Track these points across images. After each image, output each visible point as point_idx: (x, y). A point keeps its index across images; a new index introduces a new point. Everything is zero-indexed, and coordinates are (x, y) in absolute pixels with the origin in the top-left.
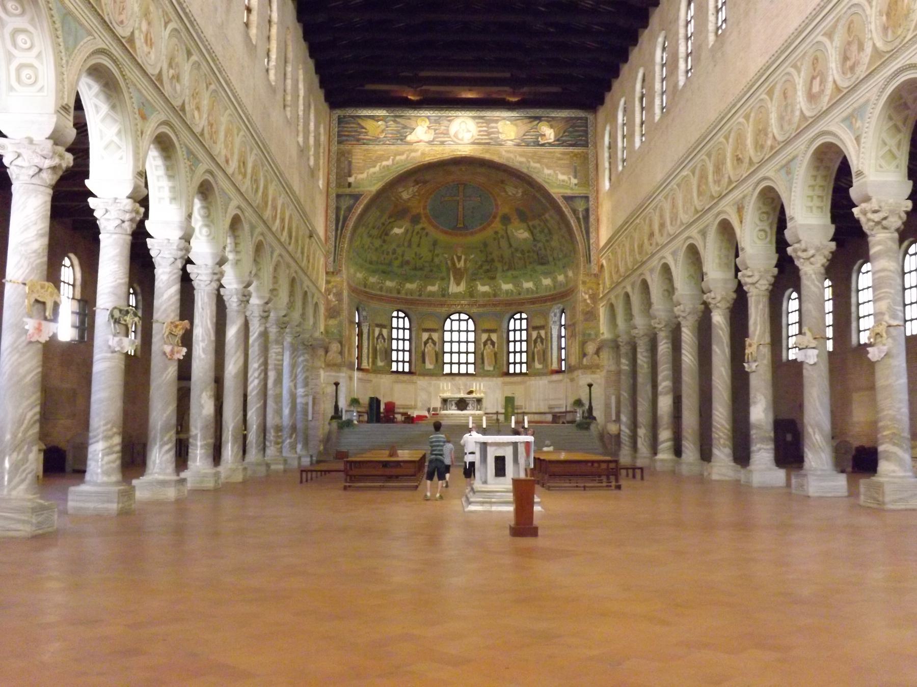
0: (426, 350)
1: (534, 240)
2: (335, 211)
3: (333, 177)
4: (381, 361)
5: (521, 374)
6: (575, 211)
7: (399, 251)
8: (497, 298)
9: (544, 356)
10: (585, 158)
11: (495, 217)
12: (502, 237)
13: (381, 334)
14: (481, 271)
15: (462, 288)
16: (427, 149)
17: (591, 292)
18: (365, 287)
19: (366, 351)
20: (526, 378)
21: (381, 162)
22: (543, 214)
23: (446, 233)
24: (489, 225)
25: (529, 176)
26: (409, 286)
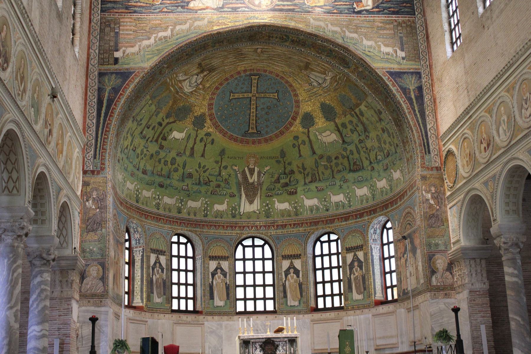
1: (344, 141)
2: (96, 93)
3: (95, 52)
4: (159, 298)
5: (333, 308)
6: (405, 91)
7: (180, 160)
8: (300, 217)
9: (364, 283)
10: (412, 28)
11: (294, 119)
12: (304, 143)
13: (158, 261)
14: (278, 185)
15: (255, 206)
16: (215, 17)
17: (433, 189)
18: (137, 202)
19: (139, 283)
20: (342, 313)
22: (358, 105)
23: (236, 140)
24: (287, 129)
26: (191, 204)
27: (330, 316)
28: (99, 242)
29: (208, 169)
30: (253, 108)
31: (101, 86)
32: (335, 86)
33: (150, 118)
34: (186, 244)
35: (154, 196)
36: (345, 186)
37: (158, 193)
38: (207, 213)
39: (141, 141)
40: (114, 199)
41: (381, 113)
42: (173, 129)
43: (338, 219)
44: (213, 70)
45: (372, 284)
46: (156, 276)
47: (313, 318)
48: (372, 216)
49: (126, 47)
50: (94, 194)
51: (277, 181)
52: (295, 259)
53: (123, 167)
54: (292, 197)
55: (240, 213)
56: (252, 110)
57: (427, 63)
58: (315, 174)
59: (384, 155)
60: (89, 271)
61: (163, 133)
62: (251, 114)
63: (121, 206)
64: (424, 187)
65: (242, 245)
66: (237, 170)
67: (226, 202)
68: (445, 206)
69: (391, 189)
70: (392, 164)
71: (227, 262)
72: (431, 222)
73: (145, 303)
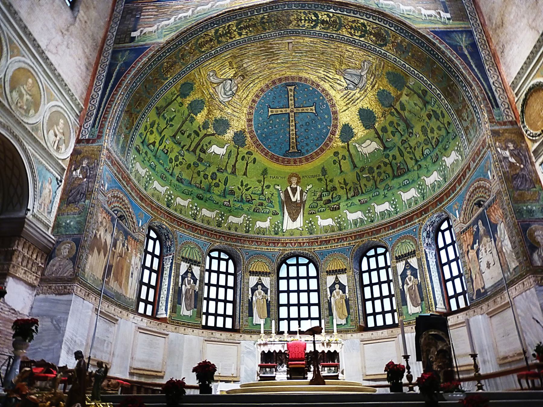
0: (254, 299)
1: (385, 148)
5: (385, 327)
8: (344, 231)
11: (333, 133)
12: (344, 158)
13: (189, 271)
14: (321, 203)
15: (299, 223)
17: (511, 146)
18: (168, 206)
19: (166, 293)
21: (178, 15)
23: (277, 160)
24: (327, 145)
25: (380, 13)
27: (383, 335)
29: (251, 188)
30: (292, 126)
31: (113, 62)
32: (372, 82)
33: (183, 123)
34: (227, 261)
35: (191, 206)
36: (389, 194)
37: (196, 204)
39: (175, 146)
41: (425, 92)
42: (212, 143)
43: (385, 228)
44: (247, 75)
45: (431, 293)
46: (186, 286)
47: (362, 337)
48: (423, 217)
49: (145, 28)
50: (84, 162)
54: (335, 213)
55: (282, 230)
56: (291, 128)
57: (478, 22)
59: (433, 146)
60: (59, 250)
61: (201, 145)
62: (291, 132)
63: (142, 201)
64: (497, 144)
65: (287, 264)
68: (533, 164)
69: (445, 179)
70: (443, 151)
73: (168, 313)
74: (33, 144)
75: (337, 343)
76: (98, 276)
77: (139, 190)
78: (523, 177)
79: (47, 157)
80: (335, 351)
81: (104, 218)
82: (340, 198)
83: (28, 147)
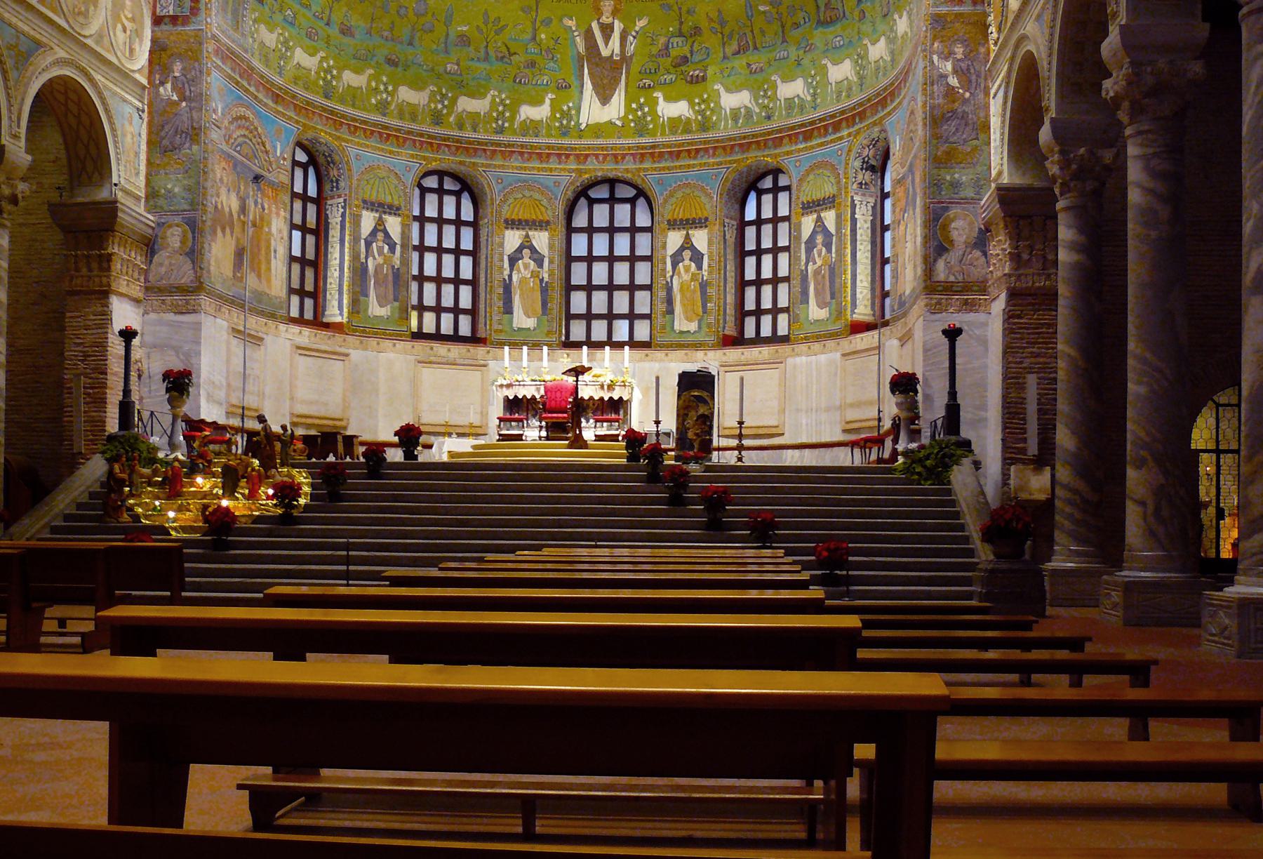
0: (515, 278)
4: (381, 306)
9: (832, 282)
13: (380, 227)
14: (666, 62)
15: (615, 110)
17: (959, 51)
18: (327, 97)
19: (336, 274)
20: (784, 349)
26: (466, 104)
28: (186, 175)
34: (458, 194)
35: (374, 84)
37: (385, 79)
38: (503, 124)
40: (237, 83)
43: (789, 136)
46: (374, 258)
47: (724, 359)
48: (856, 127)
50: (175, 68)
51: (664, 52)
52: (696, 227)
53: (278, 17)
58: (745, 34)
64: (936, 45)
66: (574, 29)
67: (548, 101)
69: (893, 60)
71: (546, 234)
72: (946, 130)
73: (346, 315)
74: (103, 68)
75: (625, 386)
76: (228, 274)
77: (268, 81)
78: (963, 117)
79: (120, 80)
80: (621, 398)
81: (224, 169)
82: (708, 55)
83: (98, 77)
